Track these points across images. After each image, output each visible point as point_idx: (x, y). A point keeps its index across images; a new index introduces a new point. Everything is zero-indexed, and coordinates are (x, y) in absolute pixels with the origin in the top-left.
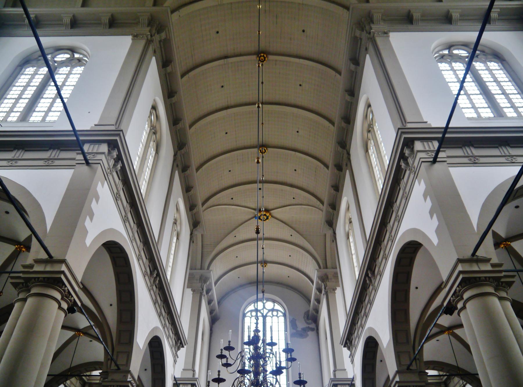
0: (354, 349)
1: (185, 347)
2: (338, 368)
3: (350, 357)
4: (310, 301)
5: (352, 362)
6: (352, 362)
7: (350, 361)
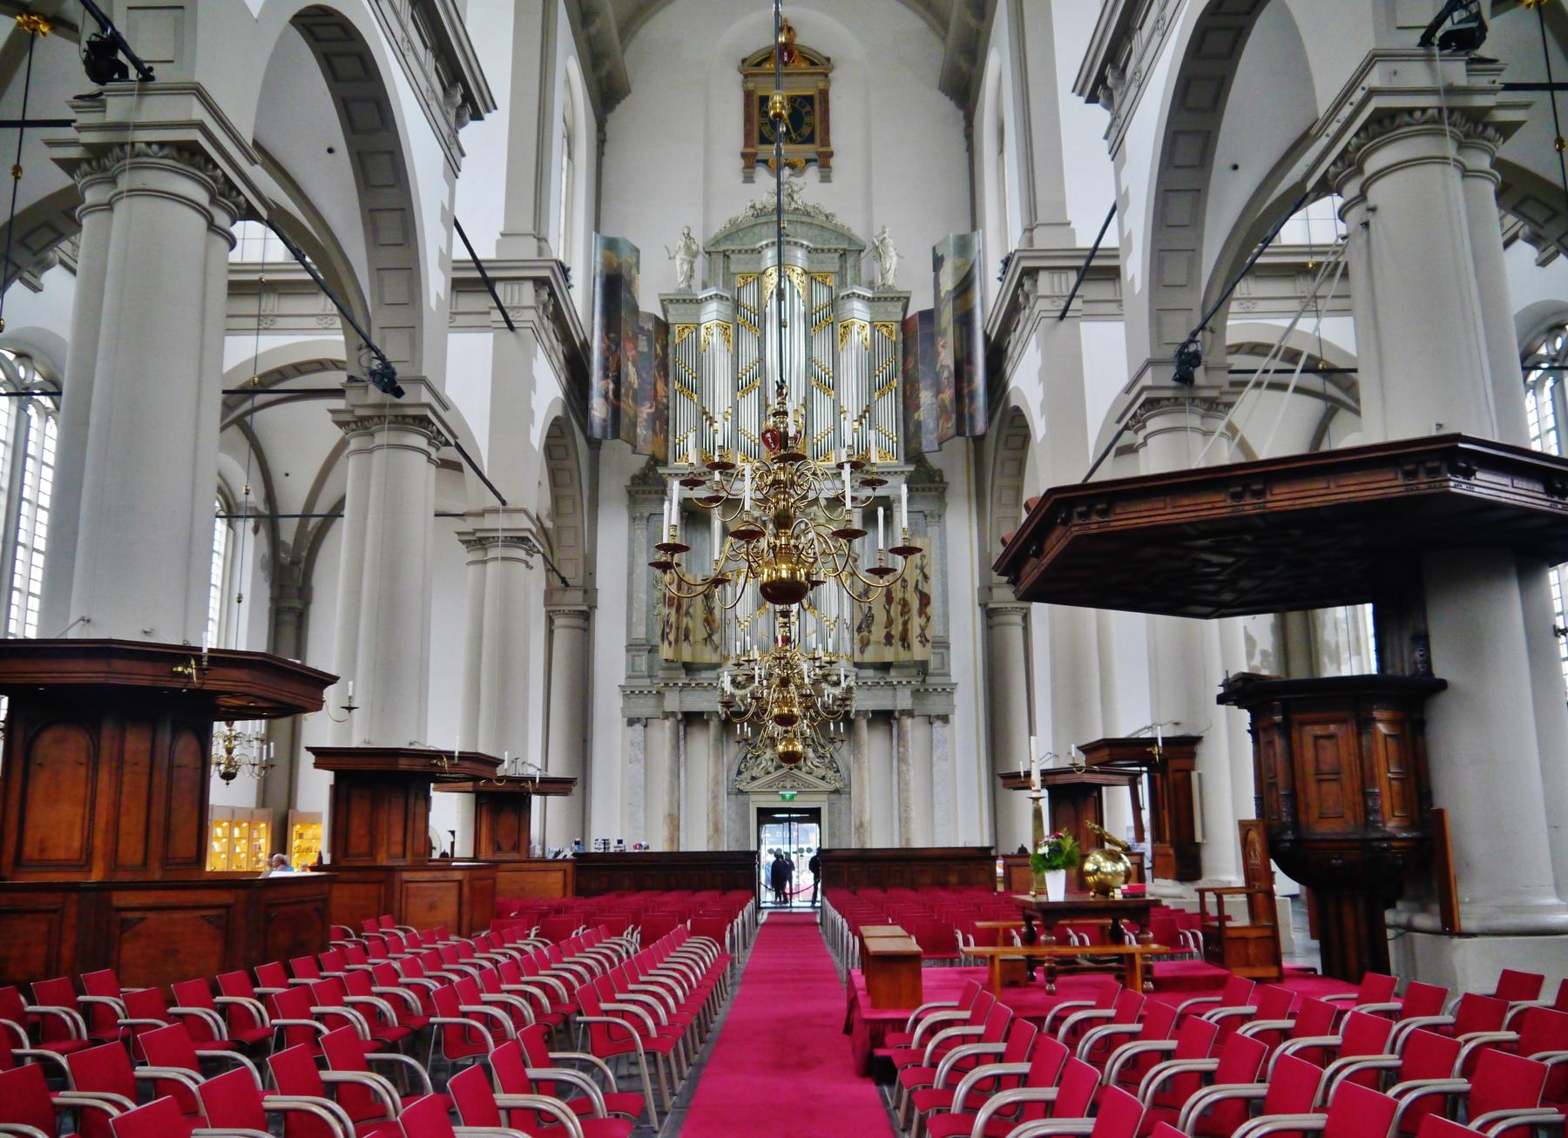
1: (487, 116)
2: (1043, 216)
3: (1106, 137)
4: (945, 24)
5: (1116, 150)
6: (1113, 152)
7: (1107, 151)
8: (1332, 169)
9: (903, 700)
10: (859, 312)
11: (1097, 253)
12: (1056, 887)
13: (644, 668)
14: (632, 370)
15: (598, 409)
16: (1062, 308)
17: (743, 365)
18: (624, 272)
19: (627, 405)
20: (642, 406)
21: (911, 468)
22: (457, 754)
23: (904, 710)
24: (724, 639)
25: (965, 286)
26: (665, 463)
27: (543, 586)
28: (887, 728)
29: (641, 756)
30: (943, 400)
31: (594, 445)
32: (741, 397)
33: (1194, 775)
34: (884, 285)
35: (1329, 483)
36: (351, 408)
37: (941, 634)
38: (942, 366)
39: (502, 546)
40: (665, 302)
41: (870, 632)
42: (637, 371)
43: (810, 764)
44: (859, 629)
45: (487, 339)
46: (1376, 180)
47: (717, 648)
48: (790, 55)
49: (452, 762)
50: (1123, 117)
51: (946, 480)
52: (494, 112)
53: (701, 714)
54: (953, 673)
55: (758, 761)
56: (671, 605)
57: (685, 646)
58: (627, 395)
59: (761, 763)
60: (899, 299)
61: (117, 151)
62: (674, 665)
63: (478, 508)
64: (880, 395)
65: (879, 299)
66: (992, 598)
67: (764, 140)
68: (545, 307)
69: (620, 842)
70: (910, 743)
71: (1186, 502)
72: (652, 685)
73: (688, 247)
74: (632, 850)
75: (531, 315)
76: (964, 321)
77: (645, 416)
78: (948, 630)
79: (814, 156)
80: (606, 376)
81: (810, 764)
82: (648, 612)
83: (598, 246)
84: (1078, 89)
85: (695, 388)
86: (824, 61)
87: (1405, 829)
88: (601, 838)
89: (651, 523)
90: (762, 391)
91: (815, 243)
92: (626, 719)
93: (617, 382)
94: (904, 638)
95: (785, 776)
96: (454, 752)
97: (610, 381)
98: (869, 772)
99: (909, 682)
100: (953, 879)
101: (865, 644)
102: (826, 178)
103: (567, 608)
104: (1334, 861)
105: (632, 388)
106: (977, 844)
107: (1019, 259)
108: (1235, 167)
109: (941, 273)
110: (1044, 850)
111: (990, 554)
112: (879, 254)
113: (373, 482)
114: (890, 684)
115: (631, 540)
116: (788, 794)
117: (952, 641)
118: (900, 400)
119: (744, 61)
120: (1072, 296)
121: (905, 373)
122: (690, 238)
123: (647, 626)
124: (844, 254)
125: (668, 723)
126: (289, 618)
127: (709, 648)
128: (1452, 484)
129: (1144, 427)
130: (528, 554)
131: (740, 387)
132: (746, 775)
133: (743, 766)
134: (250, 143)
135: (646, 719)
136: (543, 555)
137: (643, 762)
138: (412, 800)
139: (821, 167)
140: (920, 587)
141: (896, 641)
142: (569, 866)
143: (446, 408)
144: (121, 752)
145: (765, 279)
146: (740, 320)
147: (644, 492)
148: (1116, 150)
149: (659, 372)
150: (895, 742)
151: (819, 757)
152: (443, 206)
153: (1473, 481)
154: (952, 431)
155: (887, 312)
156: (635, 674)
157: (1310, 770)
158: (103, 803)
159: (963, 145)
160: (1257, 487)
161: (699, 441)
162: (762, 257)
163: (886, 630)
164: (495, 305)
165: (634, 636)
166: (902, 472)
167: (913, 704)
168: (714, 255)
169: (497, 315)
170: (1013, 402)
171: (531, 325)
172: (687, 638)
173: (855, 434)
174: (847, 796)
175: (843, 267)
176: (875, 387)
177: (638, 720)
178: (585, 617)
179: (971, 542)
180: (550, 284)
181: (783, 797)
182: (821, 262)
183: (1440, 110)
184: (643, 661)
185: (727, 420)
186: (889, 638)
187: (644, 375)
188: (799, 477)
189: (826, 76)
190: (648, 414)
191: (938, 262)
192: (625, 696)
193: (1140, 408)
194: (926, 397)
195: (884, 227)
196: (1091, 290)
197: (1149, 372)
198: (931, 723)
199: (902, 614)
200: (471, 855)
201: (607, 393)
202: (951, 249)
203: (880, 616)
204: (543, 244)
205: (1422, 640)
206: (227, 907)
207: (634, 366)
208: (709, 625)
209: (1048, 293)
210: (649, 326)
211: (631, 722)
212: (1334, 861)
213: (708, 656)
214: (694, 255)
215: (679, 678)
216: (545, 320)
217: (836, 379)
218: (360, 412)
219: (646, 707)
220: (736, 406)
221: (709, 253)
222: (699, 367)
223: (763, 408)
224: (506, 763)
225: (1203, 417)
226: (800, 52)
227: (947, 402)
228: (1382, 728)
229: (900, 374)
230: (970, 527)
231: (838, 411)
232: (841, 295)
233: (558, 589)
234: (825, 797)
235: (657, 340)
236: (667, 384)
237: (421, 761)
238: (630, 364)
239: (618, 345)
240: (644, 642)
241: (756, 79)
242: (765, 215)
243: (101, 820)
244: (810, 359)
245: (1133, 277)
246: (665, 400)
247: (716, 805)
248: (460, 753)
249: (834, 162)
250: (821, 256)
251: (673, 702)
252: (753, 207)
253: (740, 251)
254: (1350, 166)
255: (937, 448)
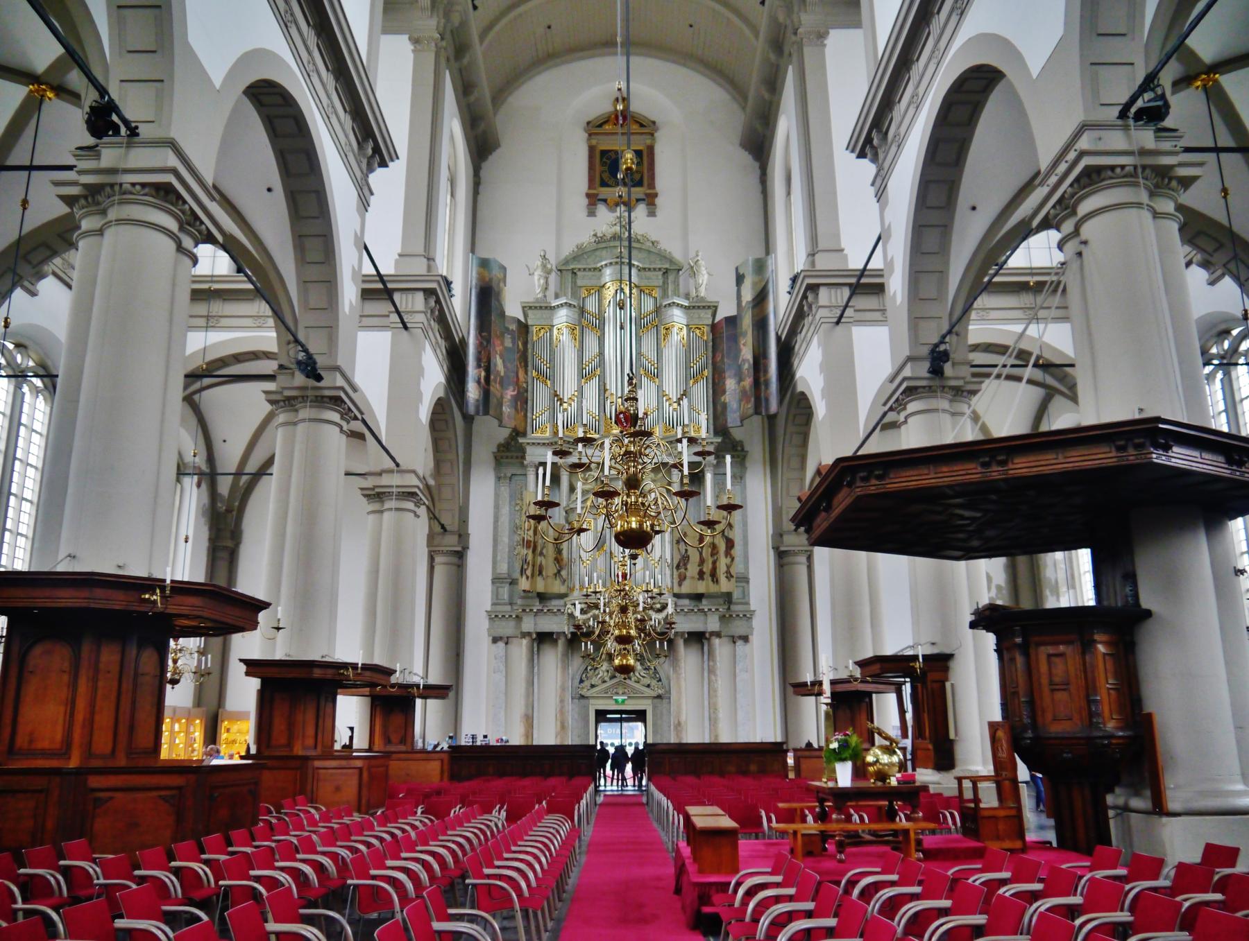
0: (894, 149)
1: (391, 164)
2: (822, 244)
3: (873, 184)
5: (881, 194)
8: (1052, 212)
9: (713, 624)
10: (678, 317)
11: (866, 273)
12: (844, 775)
13: (506, 596)
14: (499, 361)
15: (473, 392)
16: (838, 315)
17: (586, 358)
18: (494, 285)
19: (495, 388)
20: (507, 389)
21: (719, 440)
22: (360, 665)
23: (713, 632)
24: (570, 574)
25: (761, 298)
26: (524, 434)
27: (426, 531)
28: (700, 646)
29: (503, 668)
30: (744, 387)
31: (468, 419)
32: (585, 383)
33: (948, 685)
34: (697, 296)
35: (1057, 454)
36: (281, 390)
37: (743, 571)
38: (743, 360)
39: (396, 499)
40: (526, 309)
41: (686, 569)
42: (504, 362)
43: (637, 674)
44: (678, 567)
45: (387, 335)
46: (1086, 221)
47: (565, 581)
48: (625, 118)
49: (356, 672)
50: (886, 169)
51: (746, 449)
52: (397, 161)
53: (552, 634)
54: (752, 601)
55: (596, 673)
56: (528, 547)
57: (539, 580)
58: (495, 381)
59: (599, 674)
60: (709, 307)
61: (108, 189)
62: (530, 595)
63: (378, 469)
64: (694, 383)
65: (694, 307)
66: (782, 542)
67: (604, 184)
68: (432, 312)
69: (485, 737)
70: (718, 659)
71: (945, 469)
72: (512, 610)
73: (544, 266)
74: (495, 744)
75: (421, 318)
76: (761, 325)
77: (509, 397)
78: (748, 568)
79: (644, 197)
80: (479, 366)
81: (637, 674)
82: (509, 552)
83: (474, 265)
84: (851, 147)
85: (549, 376)
86: (650, 123)
87: (1121, 729)
88: (470, 733)
89: (513, 480)
90: (602, 379)
91: (643, 263)
92: (491, 638)
93: (488, 370)
94: (714, 575)
95: (618, 684)
96: (358, 664)
97: (482, 369)
98: (685, 680)
99: (717, 610)
100: (753, 768)
101: (682, 579)
102: (652, 214)
103: (445, 549)
104: (1065, 755)
105: (500, 375)
106: (772, 740)
107: (805, 277)
108: (974, 208)
109: (742, 288)
110: (834, 745)
111: (781, 507)
112: (693, 273)
113: (297, 447)
114: (702, 611)
115: (497, 496)
116: (620, 698)
117: (751, 577)
118: (710, 386)
119: (588, 123)
120: (846, 306)
121: (714, 364)
122: (546, 259)
123: (509, 563)
124: (666, 272)
125: (525, 642)
126: (225, 555)
127: (558, 582)
128: (1154, 456)
129: (905, 409)
130: (416, 505)
131: (584, 375)
132: (587, 684)
133: (584, 676)
134: (211, 185)
135: (508, 638)
136: (428, 508)
137: (504, 672)
138: (322, 703)
139: (647, 205)
140: (726, 534)
141: (707, 576)
142: (445, 756)
143: (355, 390)
144: (97, 661)
145: (605, 291)
146: (584, 322)
147: (507, 457)
148: (881, 194)
149: (520, 363)
150: (706, 657)
151: (645, 669)
152: (356, 234)
153: (1170, 454)
154: (751, 411)
155: (699, 317)
156: (499, 601)
157: (1045, 681)
158: (81, 705)
159: (759, 187)
160: (1000, 458)
161: (551, 417)
162: (601, 275)
163: (698, 568)
164: (394, 310)
165: (499, 571)
166: (712, 443)
167: (720, 627)
168: (564, 272)
169: (395, 318)
170: (800, 388)
171: (421, 325)
172: (540, 573)
173: (675, 413)
174: (667, 700)
175: (665, 283)
176: (690, 376)
177: (501, 638)
178: (460, 556)
179: (766, 498)
180: (436, 294)
181: (616, 701)
182: (648, 279)
183: (1135, 167)
184: (505, 591)
185: (574, 401)
186: (701, 575)
187: (509, 365)
188: (645, 449)
189: (652, 135)
190: (512, 396)
191: (740, 279)
192: (491, 619)
193: (901, 394)
194: (730, 384)
195: (697, 251)
196: (861, 302)
197: (909, 365)
198: (734, 642)
199: (712, 555)
200: (366, 746)
201: (479, 379)
202: (750, 269)
203: (694, 557)
204: (432, 263)
205: (1131, 578)
206: (179, 788)
207: (501, 357)
208: (558, 562)
209: (828, 304)
210: (513, 327)
211: (495, 640)
212: (1065, 755)
213: (558, 588)
214: (549, 272)
215: (534, 605)
216: (432, 322)
217: (660, 370)
218: (287, 393)
219: (507, 628)
220: (580, 390)
221: (560, 270)
222: (552, 360)
223: (602, 392)
224: (398, 673)
225: (951, 401)
226: (633, 117)
227: (748, 387)
228: (1101, 648)
229: (710, 366)
230: (765, 486)
231: (661, 394)
232: (664, 304)
233: (439, 534)
234: (649, 701)
235: (519, 339)
236: (526, 372)
237: (330, 671)
238: (498, 357)
239: (489, 341)
240: (506, 576)
241: (598, 137)
242: (605, 242)
243: (80, 717)
244: (639, 354)
245: (895, 292)
246: (525, 385)
247: (562, 707)
248: (362, 664)
249: (658, 201)
250: (648, 274)
251: (528, 624)
252: (595, 235)
253: (585, 269)
254: (1066, 209)
255: (739, 424)
